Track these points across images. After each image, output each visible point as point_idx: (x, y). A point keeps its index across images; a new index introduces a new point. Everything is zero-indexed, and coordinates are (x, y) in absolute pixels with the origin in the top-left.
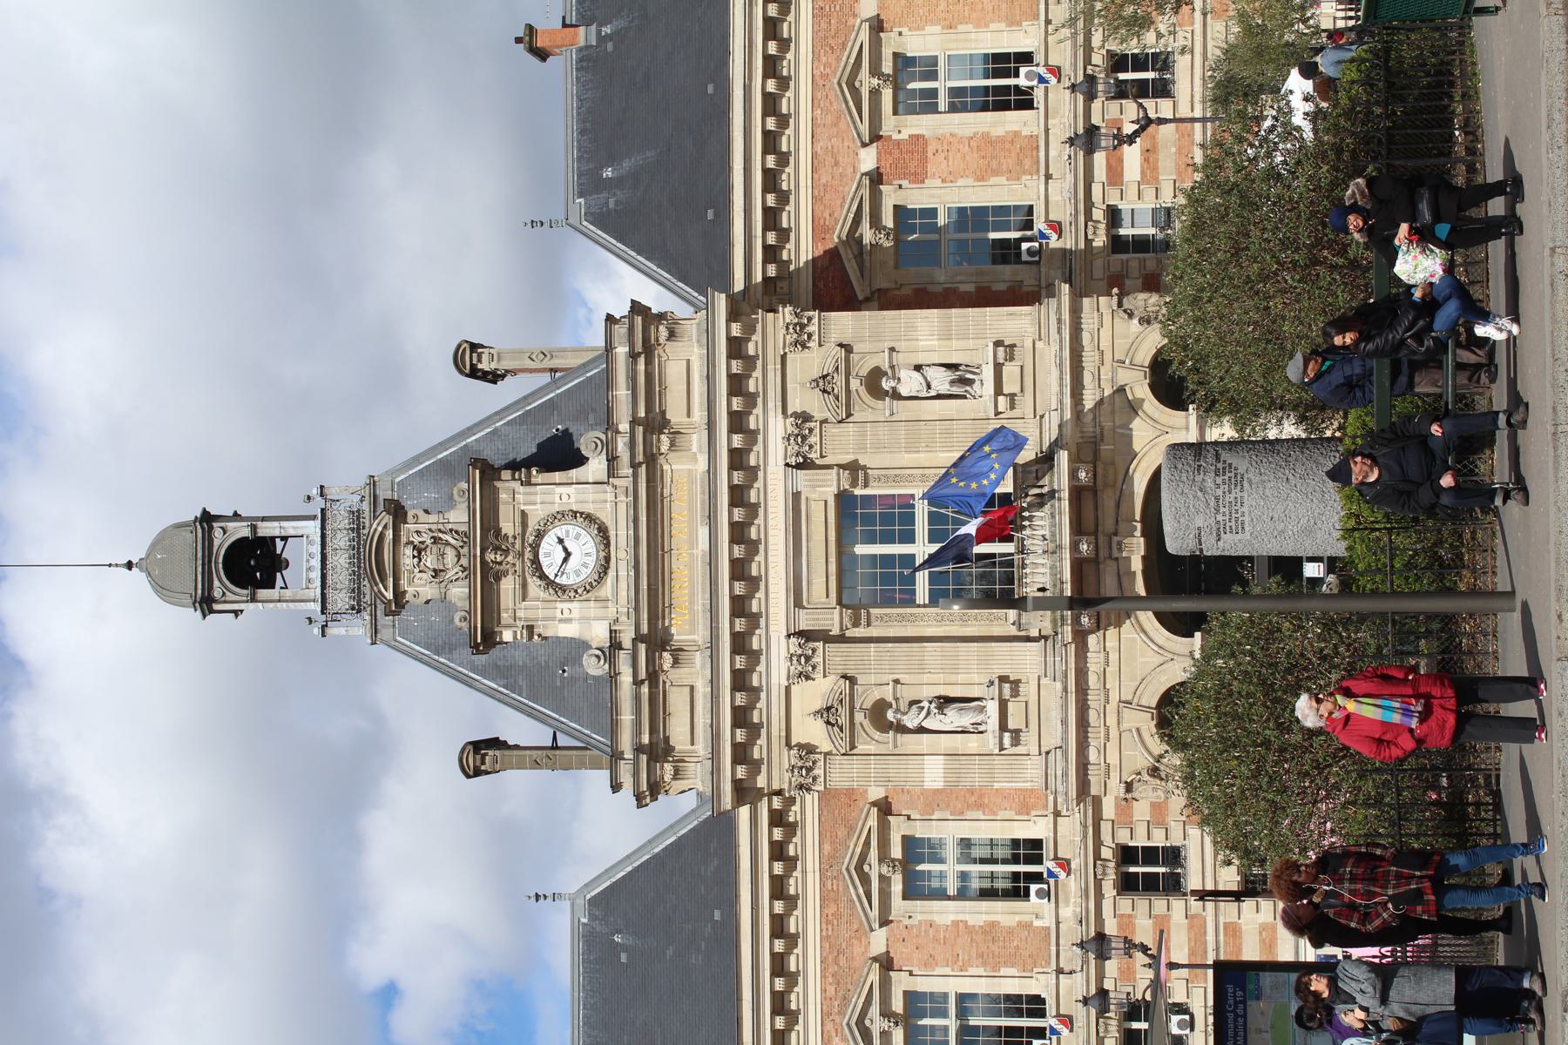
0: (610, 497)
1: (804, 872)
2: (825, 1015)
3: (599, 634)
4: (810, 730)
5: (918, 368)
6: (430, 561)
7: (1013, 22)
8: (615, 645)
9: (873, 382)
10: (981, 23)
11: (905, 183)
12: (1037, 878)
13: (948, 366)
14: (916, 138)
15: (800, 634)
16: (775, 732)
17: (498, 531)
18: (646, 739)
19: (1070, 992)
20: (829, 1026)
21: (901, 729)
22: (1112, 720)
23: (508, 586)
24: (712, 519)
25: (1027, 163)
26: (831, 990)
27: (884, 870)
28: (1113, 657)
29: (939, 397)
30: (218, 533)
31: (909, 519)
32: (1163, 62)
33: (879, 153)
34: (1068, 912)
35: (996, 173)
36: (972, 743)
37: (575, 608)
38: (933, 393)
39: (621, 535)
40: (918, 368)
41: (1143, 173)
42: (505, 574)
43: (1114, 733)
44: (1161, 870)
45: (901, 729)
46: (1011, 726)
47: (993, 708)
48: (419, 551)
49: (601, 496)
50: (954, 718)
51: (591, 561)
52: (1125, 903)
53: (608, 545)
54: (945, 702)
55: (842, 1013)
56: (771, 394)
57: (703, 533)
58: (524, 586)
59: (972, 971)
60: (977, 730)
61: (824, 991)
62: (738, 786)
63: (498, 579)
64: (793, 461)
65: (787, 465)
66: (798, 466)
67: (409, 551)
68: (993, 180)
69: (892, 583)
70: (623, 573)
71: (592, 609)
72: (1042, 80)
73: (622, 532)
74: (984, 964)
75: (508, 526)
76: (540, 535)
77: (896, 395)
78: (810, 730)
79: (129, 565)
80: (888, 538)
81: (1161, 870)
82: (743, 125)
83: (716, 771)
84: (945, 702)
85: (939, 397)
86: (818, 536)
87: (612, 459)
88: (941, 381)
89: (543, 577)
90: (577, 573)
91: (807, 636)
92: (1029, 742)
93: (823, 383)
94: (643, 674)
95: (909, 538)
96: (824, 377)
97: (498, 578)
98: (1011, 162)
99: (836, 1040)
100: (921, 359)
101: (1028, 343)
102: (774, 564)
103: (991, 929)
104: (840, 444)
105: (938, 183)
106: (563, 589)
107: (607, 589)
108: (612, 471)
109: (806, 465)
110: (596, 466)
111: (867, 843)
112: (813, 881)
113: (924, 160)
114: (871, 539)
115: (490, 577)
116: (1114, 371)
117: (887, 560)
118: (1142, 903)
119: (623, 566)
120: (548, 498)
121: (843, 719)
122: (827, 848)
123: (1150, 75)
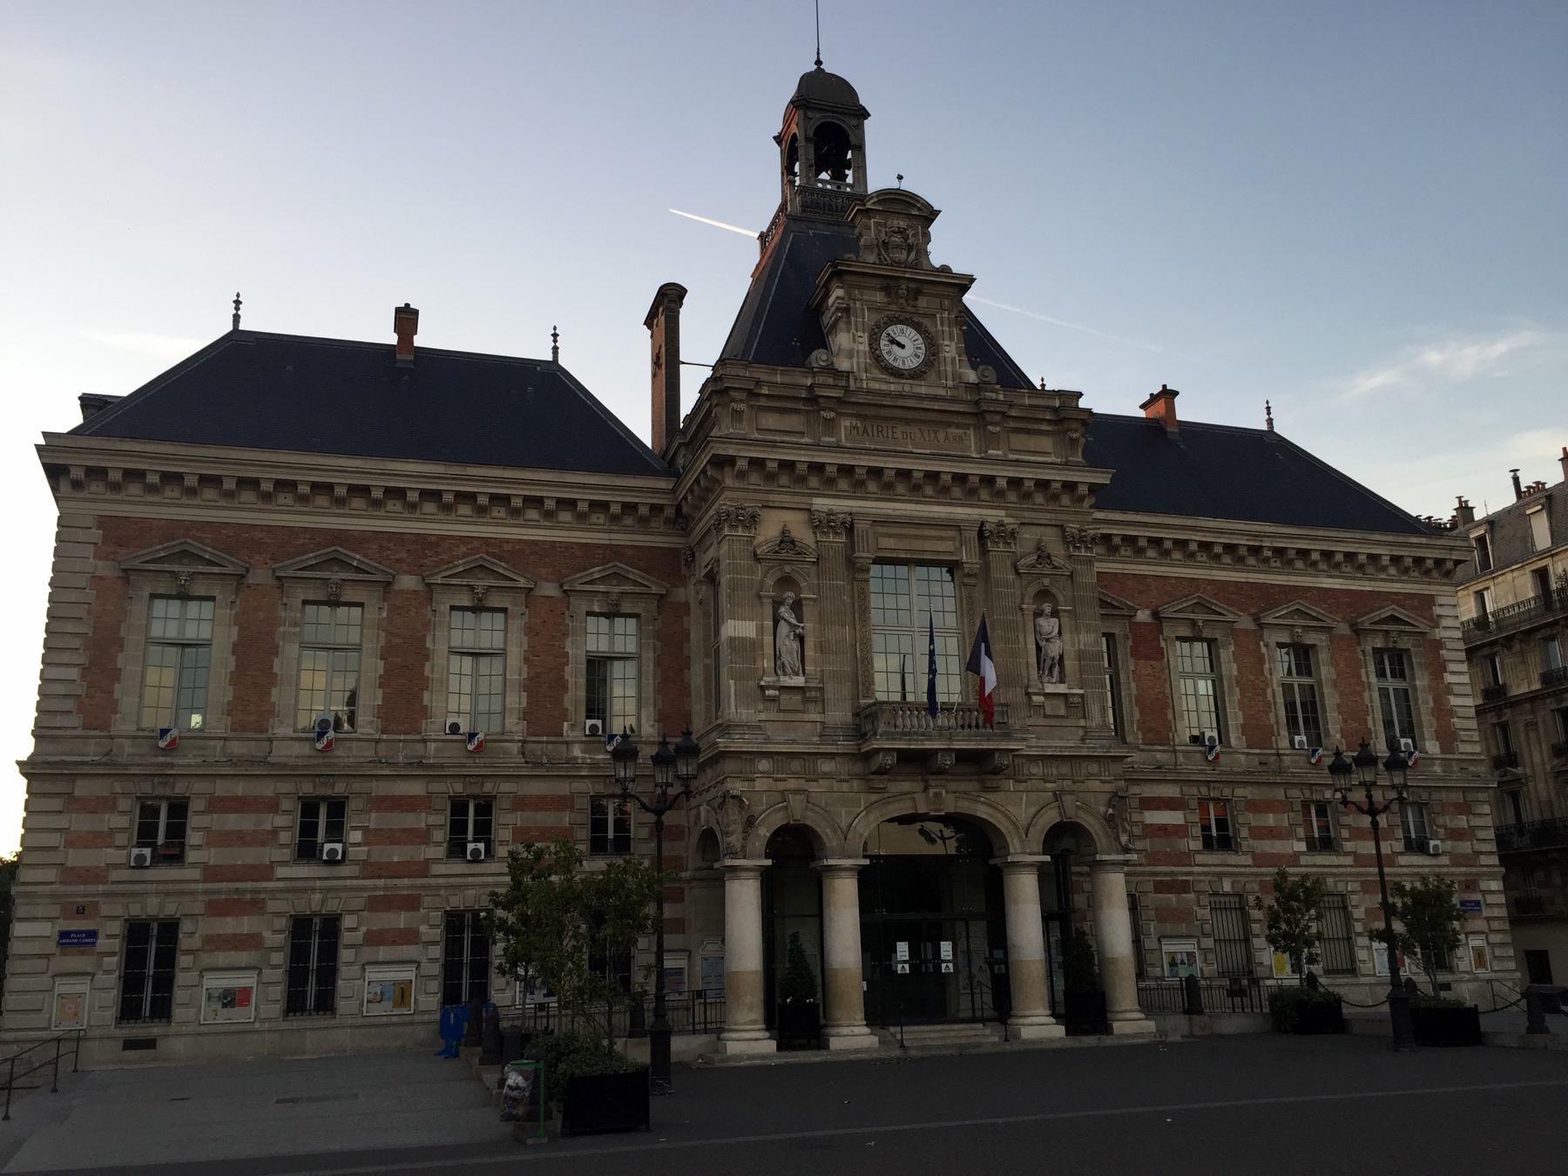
0: (950, 383)
1: (610, 531)
2: (486, 541)
3: (843, 364)
4: (770, 528)
6: (896, 239)
7: (1244, 729)
8: (837, 373)
9: (1044, 594)
10: (1242, 705)
11: (1130, 643)
13: (1061, 657)
15: (852, 524)
16: (772, 497)
17: (918, 292)
18: (765, 391)
19: (505, 752)
20: (476, 544)
21: (777, 604)
22: (792, 784)
23: (879, 297)
26: (507, 547)
27: (614, 597)
28: (845, 787)
33: (1146, 624)
34: (577, 751)
36: (768, 664)
37: (864, 347)
38: (1043, 643)
41: (1151, 825)
42: (888, 295)
43: (781, 786)
44: (611, 834)
45: (777, 604)
46: (785, 697)
47: (799, 681)
48: (901, 231)
49: (950, 375)
50: (789, 645)
51: (898, 364)
52: (585, 804)
53: (912, 378)
54: (801, 639)
55: (488, 553)
56: (1033, 515)
58: (878, 310)
59: (525, 669)
60: (779, 667)
61: (508, 541)
62: (731, 461)
63: (883, 289)
64: (987, 526)
65: (982, 524)
66: (981, 533)
67: (902, 224)
68: (1136, 711)
70: (892, 387)
71: (865, 360)
72: (1212, 748)
73: (923, 390)
74: (529, 678)
75: (922, 302)
76: (918, 327)
77: (1038, 614)
78: (770, 528)
79: (819, 62)
81: (611, 834)
82: (1170, 526)
83: (745, 441)
84: (801, 639)
85: (1039, 648)
86: (928, 545)
87: (976, 388)
88: (1054, 649)
89: (887, 325)
90: (889, 353)
91: (850, 530)
92: (773, 715)
93: (1043, 556)
94: (818, 392)
96: (1049, 557)
97: (887, 290)
99: (463, 549)
100: (1066, 636)
101: (1082, 722)
103: (562, 686)
104: (1001, 571)
105: (1132, 668)
106: (878, 340)
107: (876, 373)
108: (970, 387)
110: (972, 377)
111: (635, 583)
112: (601, 538)
113: (1147, 658)
116: (1072, 792)
118: (586, 818)
119: (899, 388)
120: (947, 335)
121: (784, 555)
122: (630, 552)
123: (1214, 833)
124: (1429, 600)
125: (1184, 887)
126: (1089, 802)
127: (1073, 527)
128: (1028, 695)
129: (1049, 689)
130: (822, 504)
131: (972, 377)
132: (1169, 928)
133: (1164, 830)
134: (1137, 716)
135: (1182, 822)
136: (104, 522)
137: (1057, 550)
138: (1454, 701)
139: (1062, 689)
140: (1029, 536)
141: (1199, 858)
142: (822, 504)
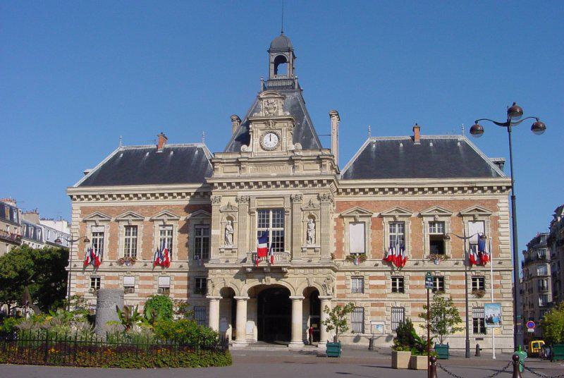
2: (168, 206)
5: (315, 228)
12: (200, 258)
14: (382, 227)
23: (263, 126)
24: (260, 177)
25: (375, 256)
29: (308, 234)
30: (287, 53)
31: (263, 227)
32: (402, 290)
35: (373, 248)
39: (275, 154)
40: (315, 228)
57: (275, 174)
66: (291, 198)
69: (263, 222)
75: (278, 125)
80: (274, 221)
85: (308, 234)
95: (274, 226)
98: (375, 251)
102: (265, 192)
107: (262, 151)
109: (291, 199)
114: (274, 216)
115: (266, 121)
117: (268, 221)
121: (228, 210)
124: (496, 201)
125: (382, 305)
126: (316, 280)
127: (321, 195)
128: (302, 248)
129: (309, 246)
130: (240, 194)
131: (293, 147)
132: (375, 318)
133: (377, 287)
134: (371, 249)
135: (384, 284)
136: (82, 208)
137: (317, 202)
138: (501, 238)
139: (313, 246)
140: (306, 199)
141: (389, 296)
142: (240, 194)
